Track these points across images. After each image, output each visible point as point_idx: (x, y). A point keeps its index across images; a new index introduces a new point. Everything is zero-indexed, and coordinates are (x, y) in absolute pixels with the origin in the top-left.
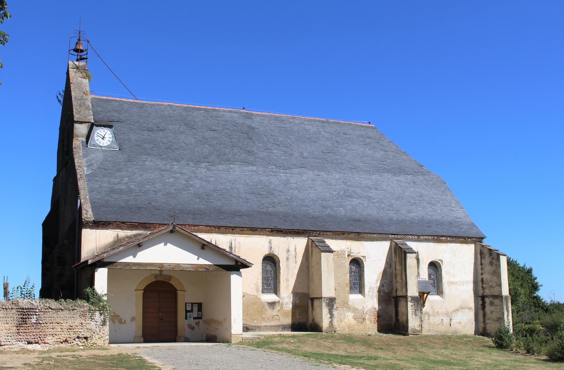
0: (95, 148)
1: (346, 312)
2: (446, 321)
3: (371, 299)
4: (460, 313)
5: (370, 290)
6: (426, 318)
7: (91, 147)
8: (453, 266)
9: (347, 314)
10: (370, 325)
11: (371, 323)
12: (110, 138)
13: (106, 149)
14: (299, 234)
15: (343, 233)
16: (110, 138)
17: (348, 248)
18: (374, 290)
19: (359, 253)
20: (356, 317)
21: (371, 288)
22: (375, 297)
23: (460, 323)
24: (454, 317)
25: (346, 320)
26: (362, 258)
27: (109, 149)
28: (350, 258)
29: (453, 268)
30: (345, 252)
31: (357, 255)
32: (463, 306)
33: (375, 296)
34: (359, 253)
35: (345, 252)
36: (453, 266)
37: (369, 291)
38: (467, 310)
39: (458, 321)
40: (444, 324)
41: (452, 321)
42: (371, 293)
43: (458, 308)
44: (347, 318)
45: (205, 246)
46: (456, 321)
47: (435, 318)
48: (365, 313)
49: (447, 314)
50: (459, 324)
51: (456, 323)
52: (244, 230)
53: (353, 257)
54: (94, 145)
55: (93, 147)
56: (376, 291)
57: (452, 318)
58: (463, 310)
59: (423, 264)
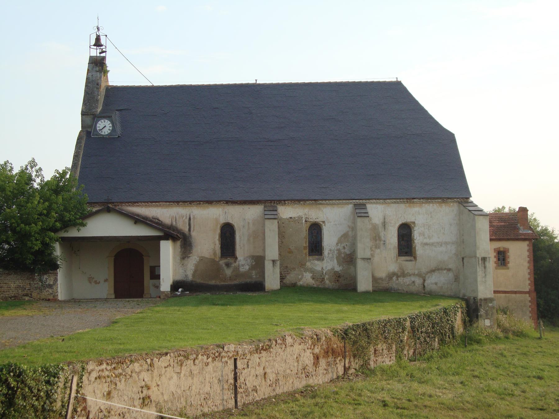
0: (98, 137)
1: (304, 273)
2: (418, 281)
3: (331, 261)
4: (436, 274)
5: (329, 252)
6: (394, 278)
7: (94, 137)
8: (429, 227)
9: (305, 274)
10: (330, 284)
11: (331, 283)
12: (110, 127)
13: (107, 137)
14: (255, 204)
15: (299, 201)
16: (110, 127)
17: (305, 214)
18: (334, 252)
19: (318, 218)
20: (315, 277)
21: (330, 250)
22: (335, 259)
23: (436, 284)
24: (429, 277)
25: (304, 280)
26: (321, 223)
27: (111, 137)
28: (309, 224)
29: (428, 229)
30: (302, 218)
31: (315, 220)
32: (440, 267)
33: (335, 257)
34: (318, 218)
35: (302, 218)
36: (429, 227)
37: (329, 253)
38: (445, 272)
39: (433, 281)
40: (416, 284)
41: (426, 282)
42: (331, 255)
43: (434, 269)
44: (305, 278)
45: (138, 220)
46: (431, 282)
47: (405, 279)
48: (324, 273)
49: (419, 275)
50: (435, 285)
51: (431, 284)
52: (200, 204)
53: (311, 223)
54: (96, 135)
55: (96, 137)
56: (337, 253)
57: (427, 278)
58: (440, 271)
59: (391, 226)
